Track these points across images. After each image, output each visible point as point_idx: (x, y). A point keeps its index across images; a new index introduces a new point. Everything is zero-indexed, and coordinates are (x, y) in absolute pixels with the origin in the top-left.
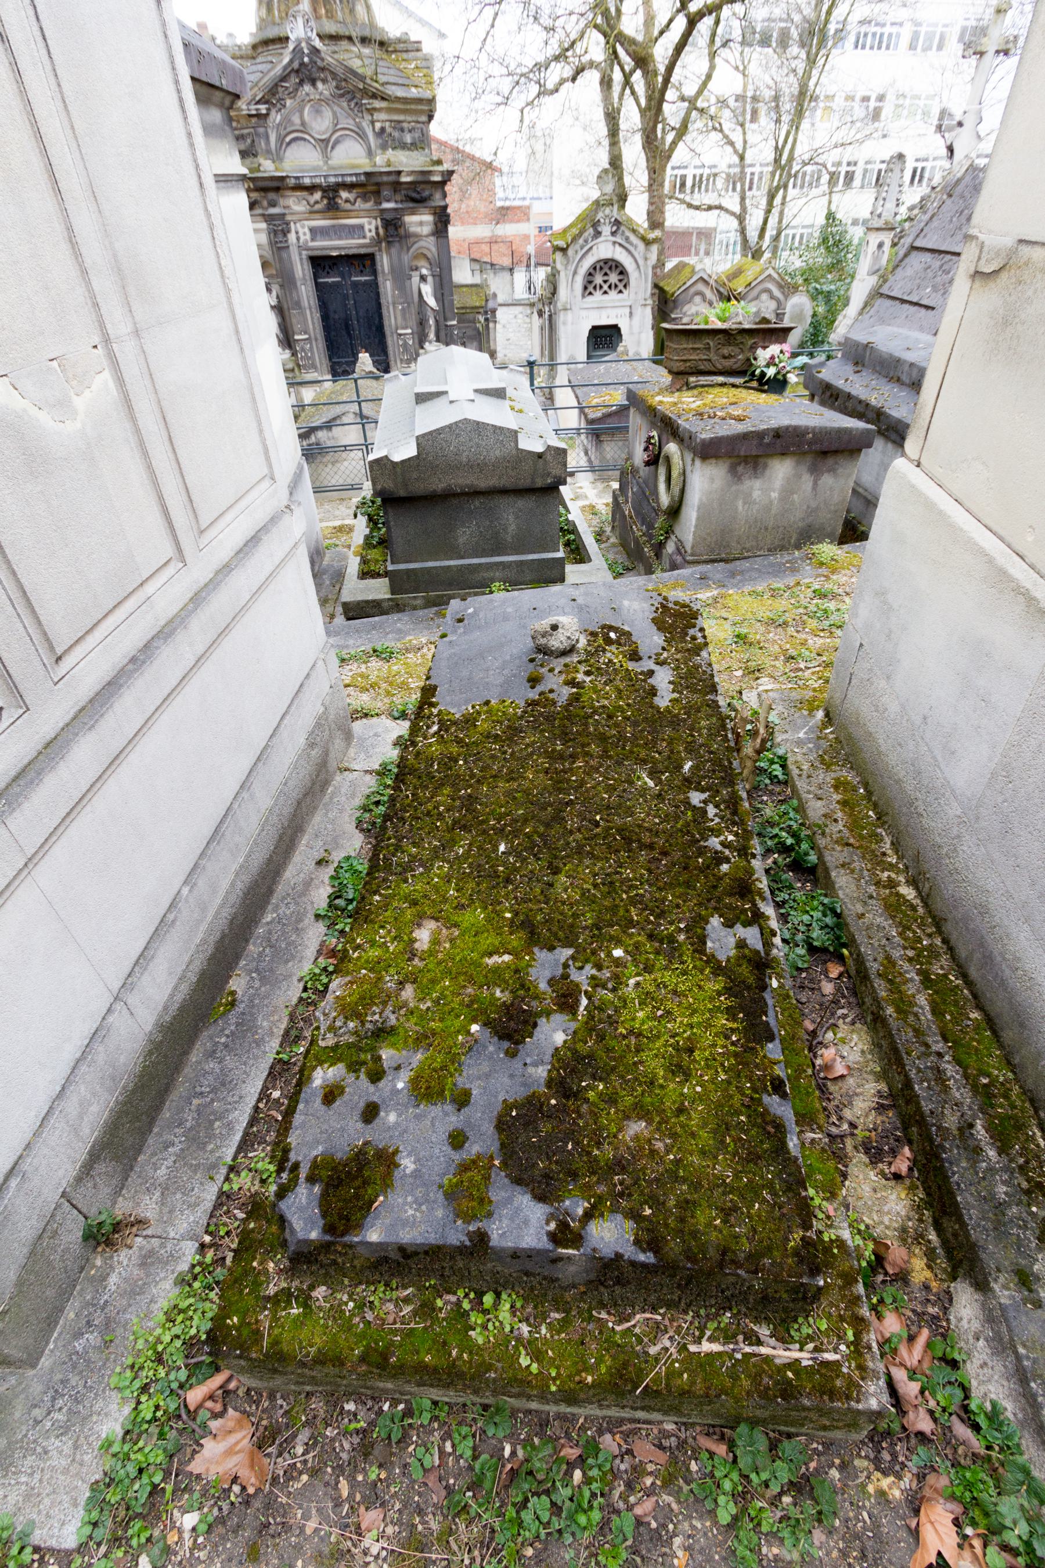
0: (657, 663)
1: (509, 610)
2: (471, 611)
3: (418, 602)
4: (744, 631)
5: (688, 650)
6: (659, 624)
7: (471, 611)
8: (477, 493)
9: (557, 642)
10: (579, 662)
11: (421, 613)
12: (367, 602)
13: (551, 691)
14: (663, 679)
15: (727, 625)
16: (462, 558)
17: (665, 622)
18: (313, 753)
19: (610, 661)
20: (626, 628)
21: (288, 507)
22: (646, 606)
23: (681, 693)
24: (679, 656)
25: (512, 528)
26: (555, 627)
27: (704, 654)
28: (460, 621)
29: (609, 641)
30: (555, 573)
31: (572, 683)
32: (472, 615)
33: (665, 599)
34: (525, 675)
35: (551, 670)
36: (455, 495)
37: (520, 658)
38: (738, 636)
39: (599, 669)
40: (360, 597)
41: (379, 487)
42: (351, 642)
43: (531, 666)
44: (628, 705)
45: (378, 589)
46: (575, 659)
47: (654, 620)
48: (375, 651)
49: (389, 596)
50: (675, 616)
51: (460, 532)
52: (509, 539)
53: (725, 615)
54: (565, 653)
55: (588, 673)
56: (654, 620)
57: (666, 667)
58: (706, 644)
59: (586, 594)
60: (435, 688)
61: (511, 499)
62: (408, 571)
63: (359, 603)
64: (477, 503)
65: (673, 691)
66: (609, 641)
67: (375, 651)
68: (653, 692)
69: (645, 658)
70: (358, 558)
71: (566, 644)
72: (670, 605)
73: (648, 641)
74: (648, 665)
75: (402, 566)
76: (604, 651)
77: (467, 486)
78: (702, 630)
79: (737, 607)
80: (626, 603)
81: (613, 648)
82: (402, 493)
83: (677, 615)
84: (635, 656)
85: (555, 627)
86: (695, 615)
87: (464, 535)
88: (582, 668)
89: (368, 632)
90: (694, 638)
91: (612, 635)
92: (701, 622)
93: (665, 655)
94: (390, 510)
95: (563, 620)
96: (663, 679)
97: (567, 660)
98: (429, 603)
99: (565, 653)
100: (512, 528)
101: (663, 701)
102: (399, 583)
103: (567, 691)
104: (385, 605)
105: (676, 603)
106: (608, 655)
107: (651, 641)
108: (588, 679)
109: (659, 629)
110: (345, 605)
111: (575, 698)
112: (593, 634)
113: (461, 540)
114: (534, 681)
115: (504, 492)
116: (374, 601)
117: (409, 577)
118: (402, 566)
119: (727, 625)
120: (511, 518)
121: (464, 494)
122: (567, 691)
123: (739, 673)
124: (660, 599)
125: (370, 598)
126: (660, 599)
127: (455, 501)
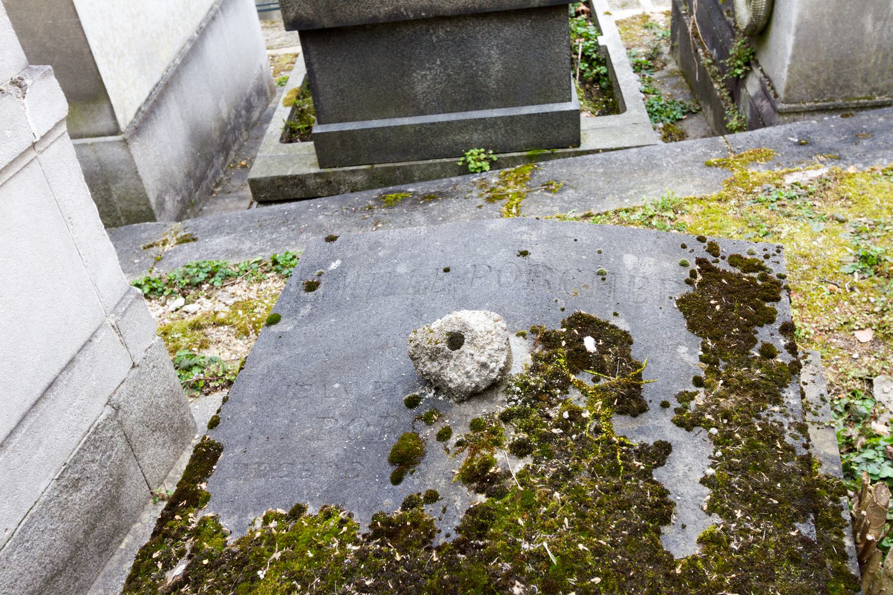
0: (680, 423)
1: (402, 269)
2: (334, 266)
3: (359, 178)
4: (876, 250)
5: (753, 386)
6: (693, 311)
7: (334, 266)
8: (440, 19)
9: (461, 371)
10: (506, 418)
11: (357, 197)
12: (285, 178)
13: (432, 497)
14: (689, 470)
15: (845, 233)
16: (423, 113)
17: (706, 308)
18: (77, 497)
19: (575, 413)
20: (622, 324)
21: (17, 83)
22: (670, 267)
23: (729, 515)
24: (728, 404)
25: (497, 68)
26: (456, 341)
27: (790, 396)
28: (311, 287)
29: (580, 360)
30: (564, 134)
31: (479, 477)
32: (341, 272)
33: (713, 249)
34: (390, 440)
35: (444, 436)
36: (407, 22)
37: (392, 391)
38: (864, 258)
39: (546, 438)
40: (275, 172)
41: (292, 15)
42: (247, 245)
43: (408, 416)
44: (598, 551)
45: (302, 160)
46: (499, 405)
47: (684, 304)
48: (275, 262)
49: (316, 170)
50: (727, 291)
51: (417, 76)
52: (493, 85)
53: (841, 213)
54: (475, 395)
55: (520, 449)
56: (684, 304)
57: (701, 433)
58: (795, 368)
59: (552, 239)
60: (219, 449)
61: (494, 25)
62: (342, 133)
63: (273, 180)
64: (441, 33)
65: (711, 510)
66: (580, 360)
67: (275, 262)
68: (661, 510)
69: (654, 406)
70: (289, 109)
71: (478, 379)
72: (723, 265)
73: (664, 359)
74: (659, 426)
75: (334, 128)
76: (565, 385)
77: (423, 8)
78: (788, 329)
79: (861, 201)
80: (629, 260)
81: (586, 378)
82: (327, 23)
83: (737, 290)
84: (631, 402)
85: (456, 341)
86: (773, 289)
87: (424, 80)
88: (511, 434)
89: (275, 229)
90: (768, 352)
91: (590, 344)
92: (786, 309)
93: (700, 399)
94: (311, 47)
95: (478, 321)
96: (689, 470)
97: (481, 410)
98: (376, 181)
99: (475, 395)
100: (497, 68)
101: (683, 542)
102: (329, 151)
103: (464, 500)
104: (311, 182)
105: (735, 260)
106: (574, 395)
107: (672, 356)
108: (517, 466)
109: (692, 327)
110: (254, 183)
111: (478, 523)
112: (548, 340)
113: (419, 88)
114: (405, 460)
115: (482, 15)
116: (294, 177)
117: (343, 142)
118: (334, 128)
119: (845, 233)
120: (495, 53)
121: (425, 20)
122: (464, 500)
123: (866, 336)
124: (701, 251)
125: (289, 173)
126: (701, 251)
127: (407, 32)
